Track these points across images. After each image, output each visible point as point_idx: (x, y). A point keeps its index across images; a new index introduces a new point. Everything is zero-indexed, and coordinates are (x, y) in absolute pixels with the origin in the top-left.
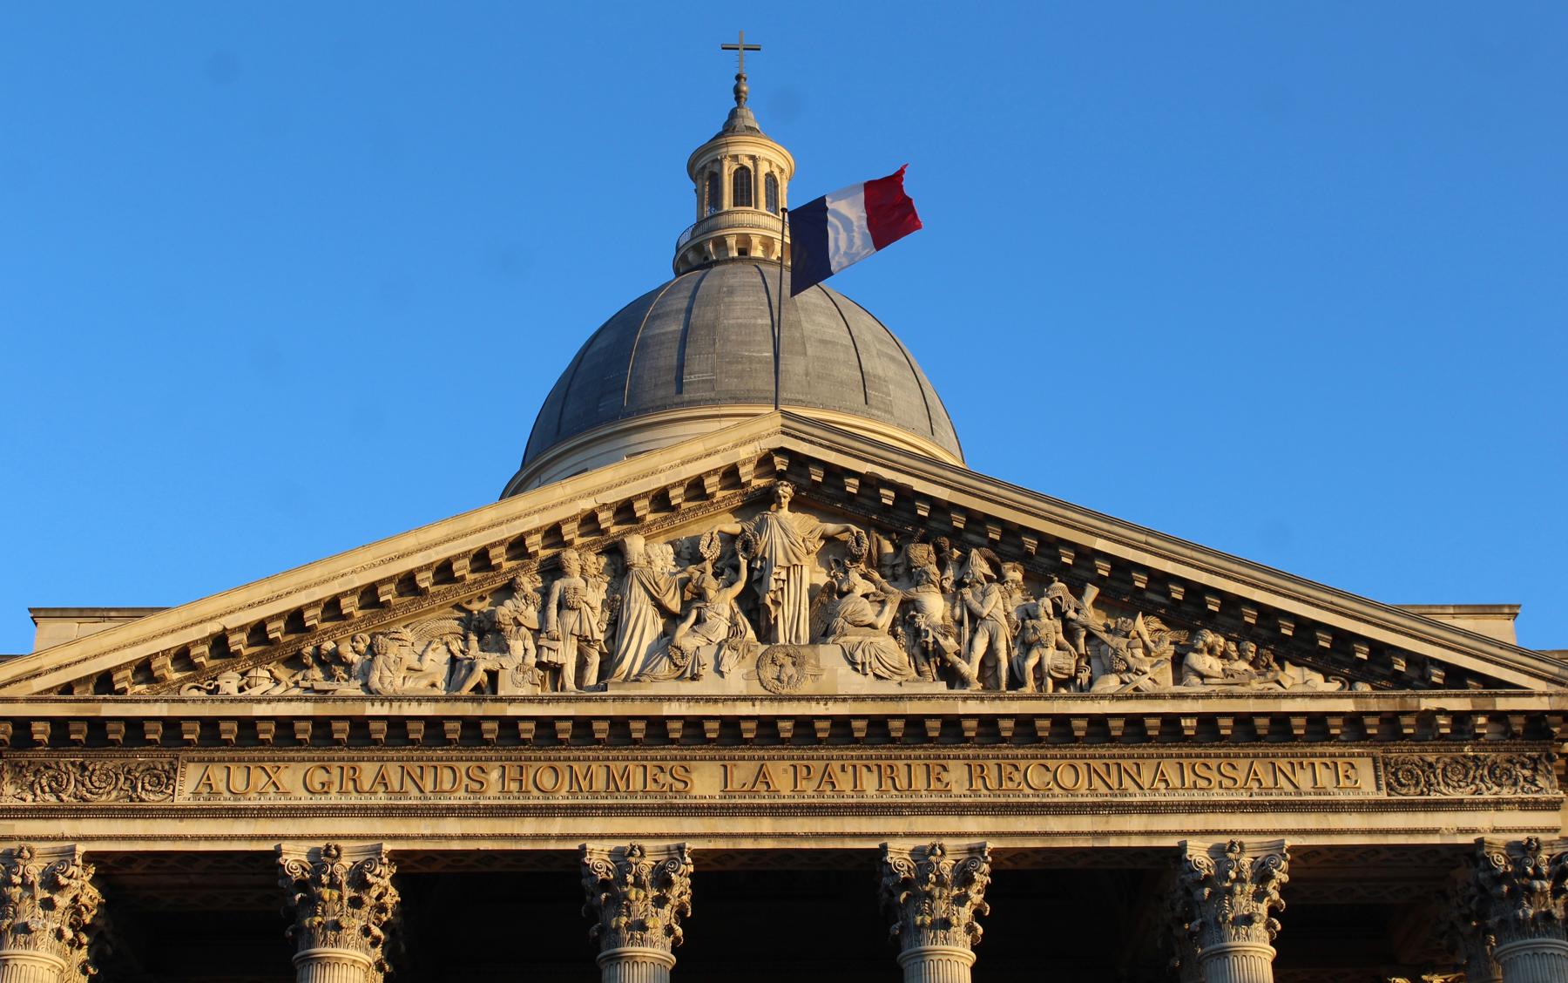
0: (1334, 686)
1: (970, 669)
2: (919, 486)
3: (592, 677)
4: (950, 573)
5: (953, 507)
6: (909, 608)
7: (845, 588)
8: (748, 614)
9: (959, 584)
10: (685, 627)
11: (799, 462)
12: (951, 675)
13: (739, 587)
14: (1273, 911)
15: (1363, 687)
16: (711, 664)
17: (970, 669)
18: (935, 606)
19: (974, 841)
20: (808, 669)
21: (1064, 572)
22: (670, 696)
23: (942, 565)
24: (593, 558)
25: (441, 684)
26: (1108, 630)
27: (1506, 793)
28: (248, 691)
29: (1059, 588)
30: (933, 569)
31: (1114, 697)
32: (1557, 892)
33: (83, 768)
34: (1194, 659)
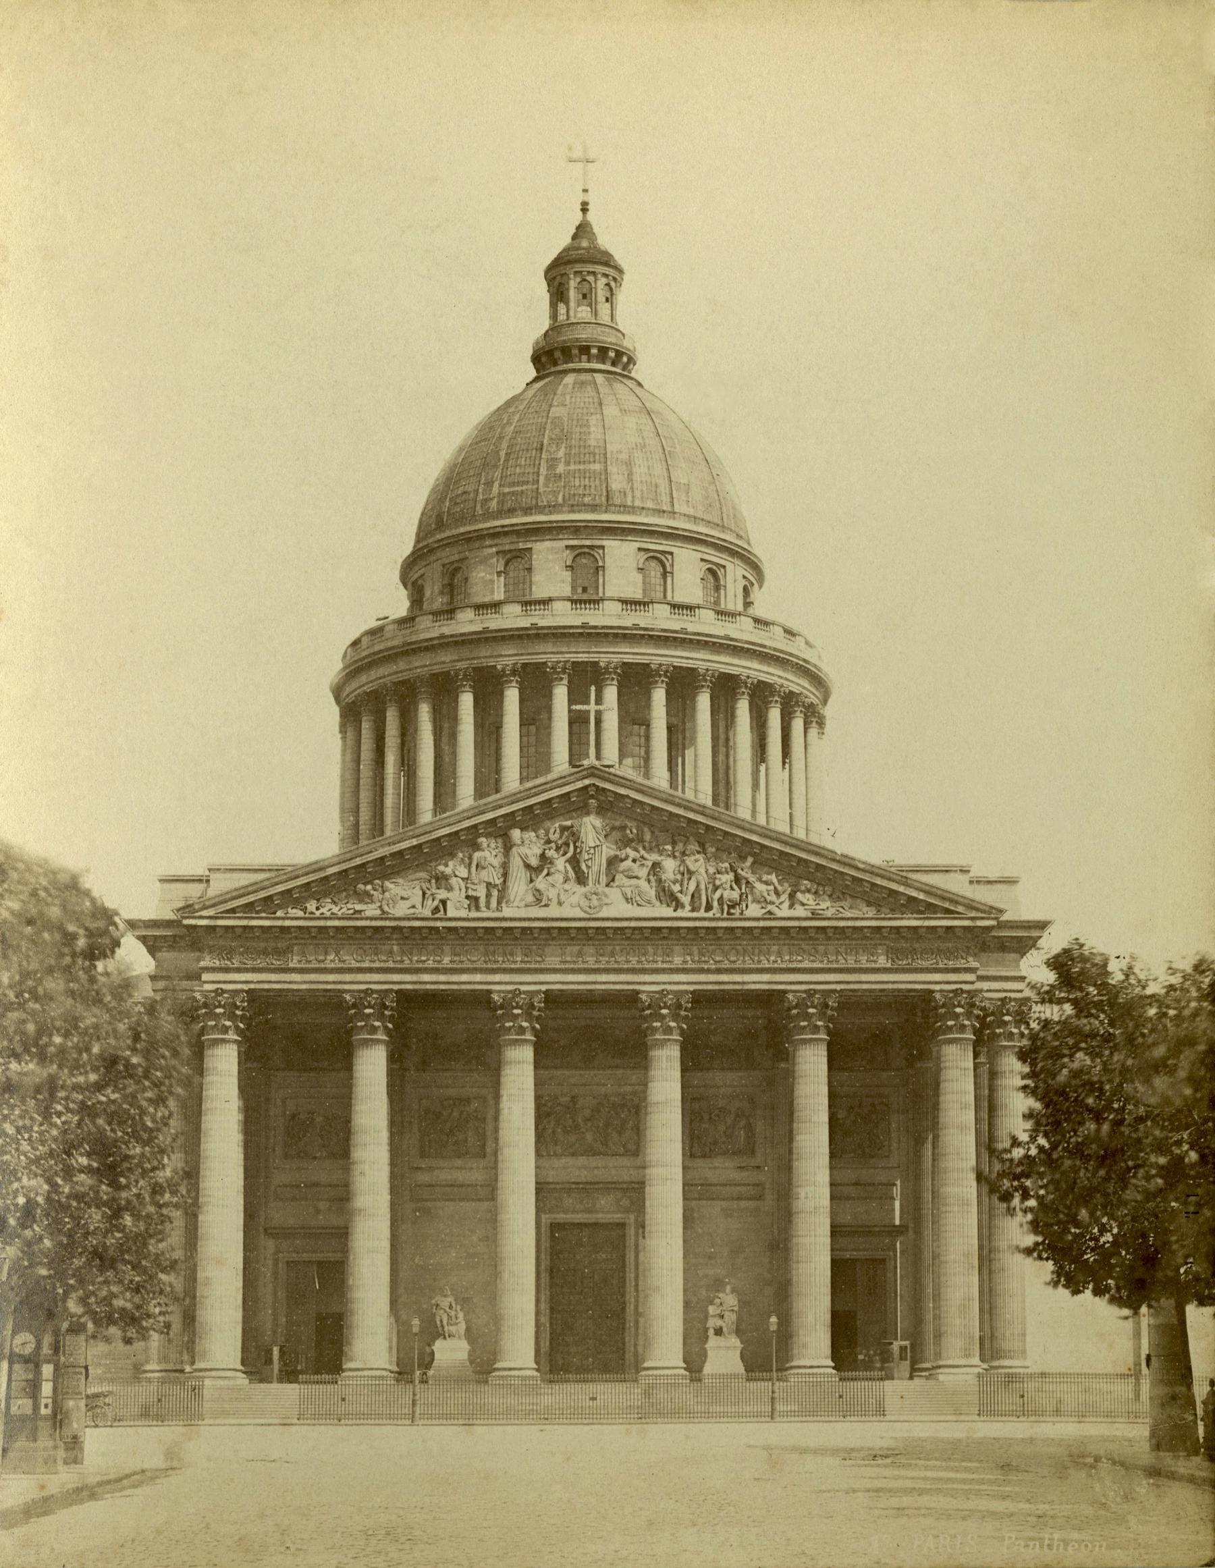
0: (871, 912)
1: (685, 899)
4: (680, 847)
7: (622, 854)
8: (573, 868)
9: (683, 854)
10: (540, 877)
12: (679, 905)
13: (569, 855)
16: (555, 901)
17: (685, 899)
18: (670, 866)
23: (674, 843)
25: (419, 905)
26: (760, 880)
28: (322, 910)
34: (799, 895)
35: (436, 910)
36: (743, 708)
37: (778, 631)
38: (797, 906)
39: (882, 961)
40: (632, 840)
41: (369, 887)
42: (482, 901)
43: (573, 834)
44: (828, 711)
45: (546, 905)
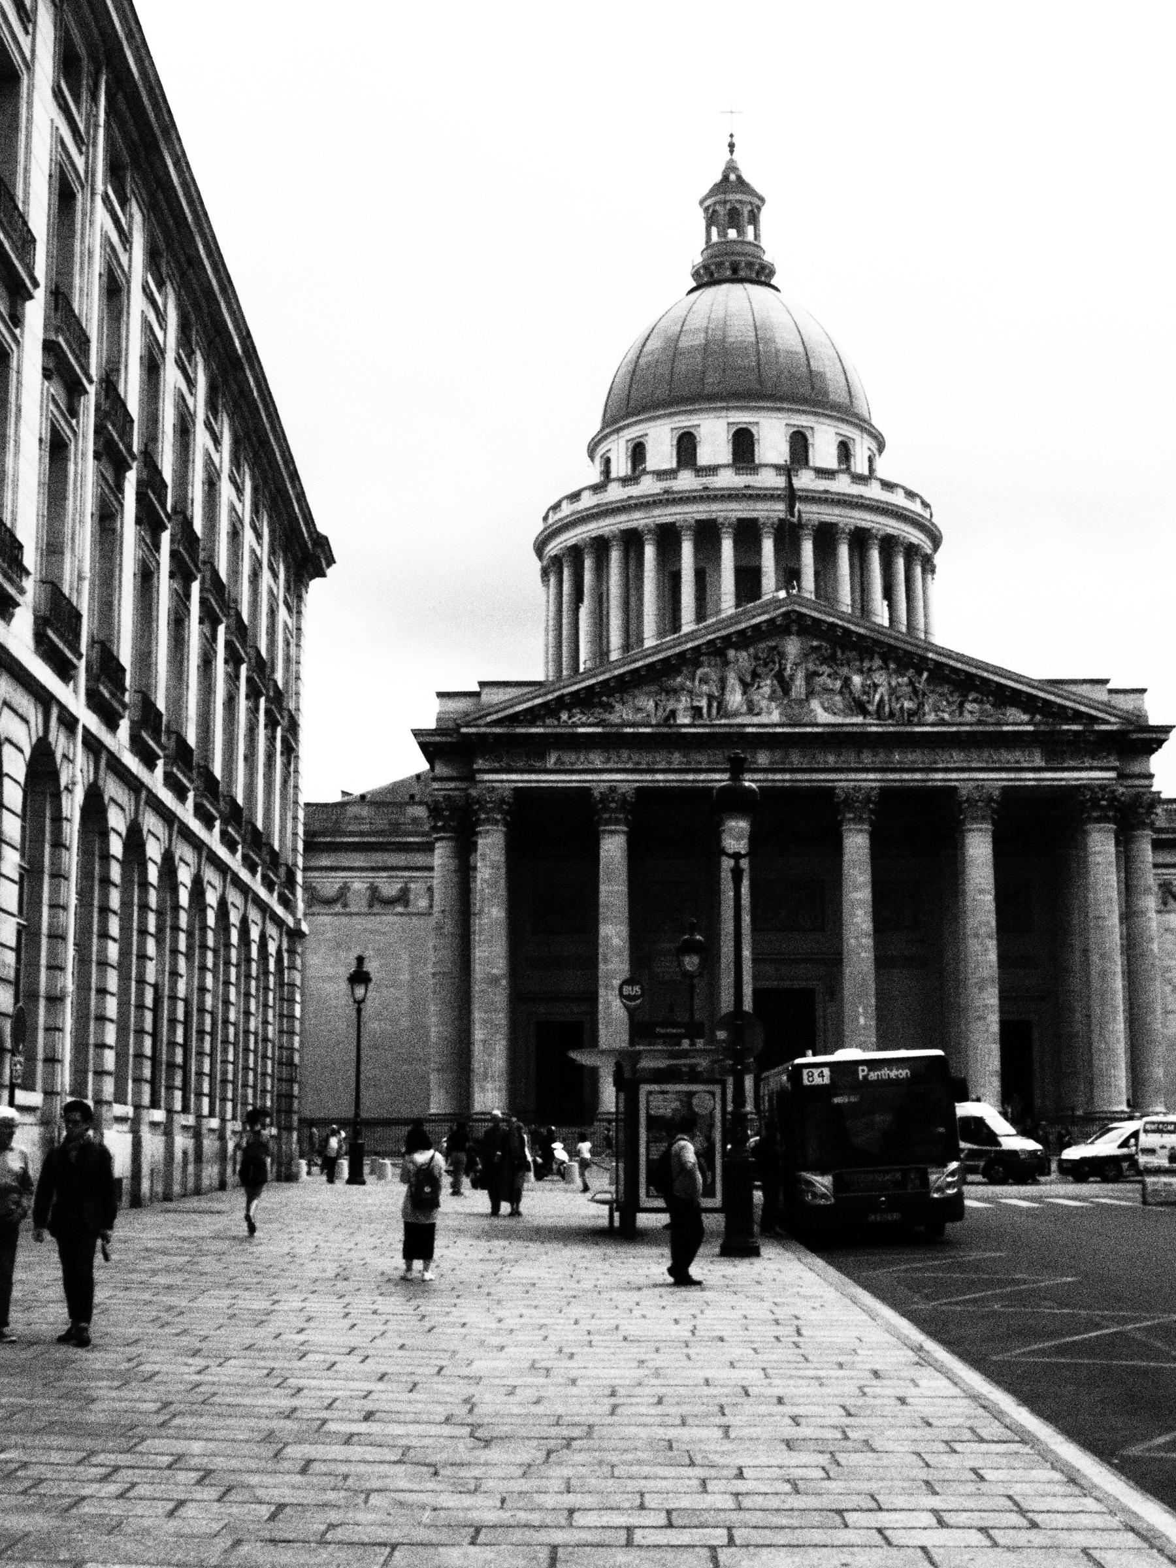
0: (1026, 718)
1: (872, 708)
2: (853, 628)
3: (714, 711)
4: (866, 664)
5: (869, 637)
6: (847, 682)
9: (870, 669)
11: (802, 616)
14: (994, 811)
15: (1038, 717)
16: (765, 709)
17: (872, 708)
18: (857, 680)
19: (874, 784)
20: (805, 710)
21: (914, 666)
22: (751, 723)
26: (932, 692)
27: (1095, 764)
29: (911, 672)
30: (858, 663)
31: (933, 725)
32: (1110, 806)
33: (508, 752)
34: (969, 706)
35: (667, 719)
36: (875, 555)
37: (901, 492)
38: (966, 714)
39: (1039, 762)
40: (825, 659)
41: (611, 700)
42: (705, 710)
43: (779, 653)
44: (938, 559)
45: (758, 714)
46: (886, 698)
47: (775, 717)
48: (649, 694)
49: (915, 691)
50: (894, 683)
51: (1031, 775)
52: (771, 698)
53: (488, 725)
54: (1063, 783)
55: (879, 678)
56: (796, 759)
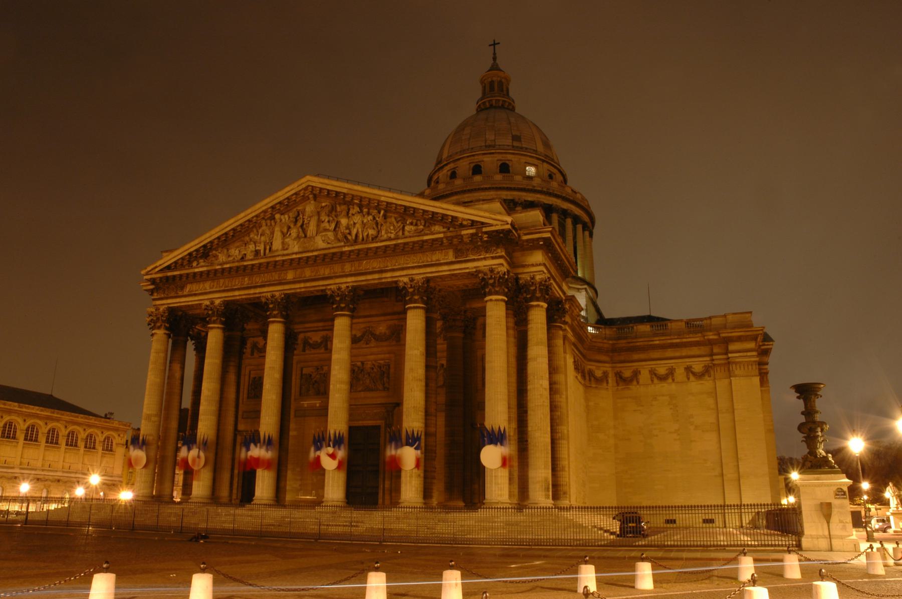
3: (267, 251)
18: (344, 221)
24: (268, 221)
34: (407, 228)
35: (242, 258)
38: (406, 233)
42: (262, 252)
46: (360, 230)
47: (296, 249)
48: (238, 247)
49: (377, 224)
50: (365, 221)
51: (445, 268)
52: (295, 239)
53: (156, 273)
54: (467, 271)
55: (357, 219)
56: (308, 273)
